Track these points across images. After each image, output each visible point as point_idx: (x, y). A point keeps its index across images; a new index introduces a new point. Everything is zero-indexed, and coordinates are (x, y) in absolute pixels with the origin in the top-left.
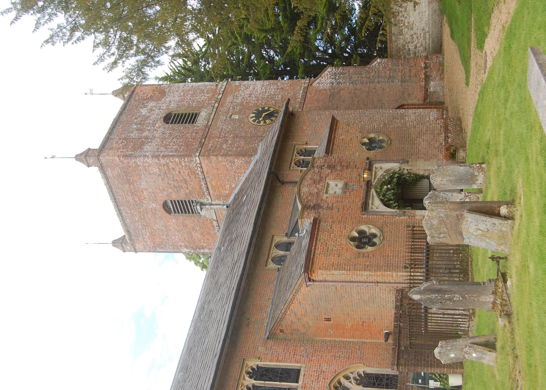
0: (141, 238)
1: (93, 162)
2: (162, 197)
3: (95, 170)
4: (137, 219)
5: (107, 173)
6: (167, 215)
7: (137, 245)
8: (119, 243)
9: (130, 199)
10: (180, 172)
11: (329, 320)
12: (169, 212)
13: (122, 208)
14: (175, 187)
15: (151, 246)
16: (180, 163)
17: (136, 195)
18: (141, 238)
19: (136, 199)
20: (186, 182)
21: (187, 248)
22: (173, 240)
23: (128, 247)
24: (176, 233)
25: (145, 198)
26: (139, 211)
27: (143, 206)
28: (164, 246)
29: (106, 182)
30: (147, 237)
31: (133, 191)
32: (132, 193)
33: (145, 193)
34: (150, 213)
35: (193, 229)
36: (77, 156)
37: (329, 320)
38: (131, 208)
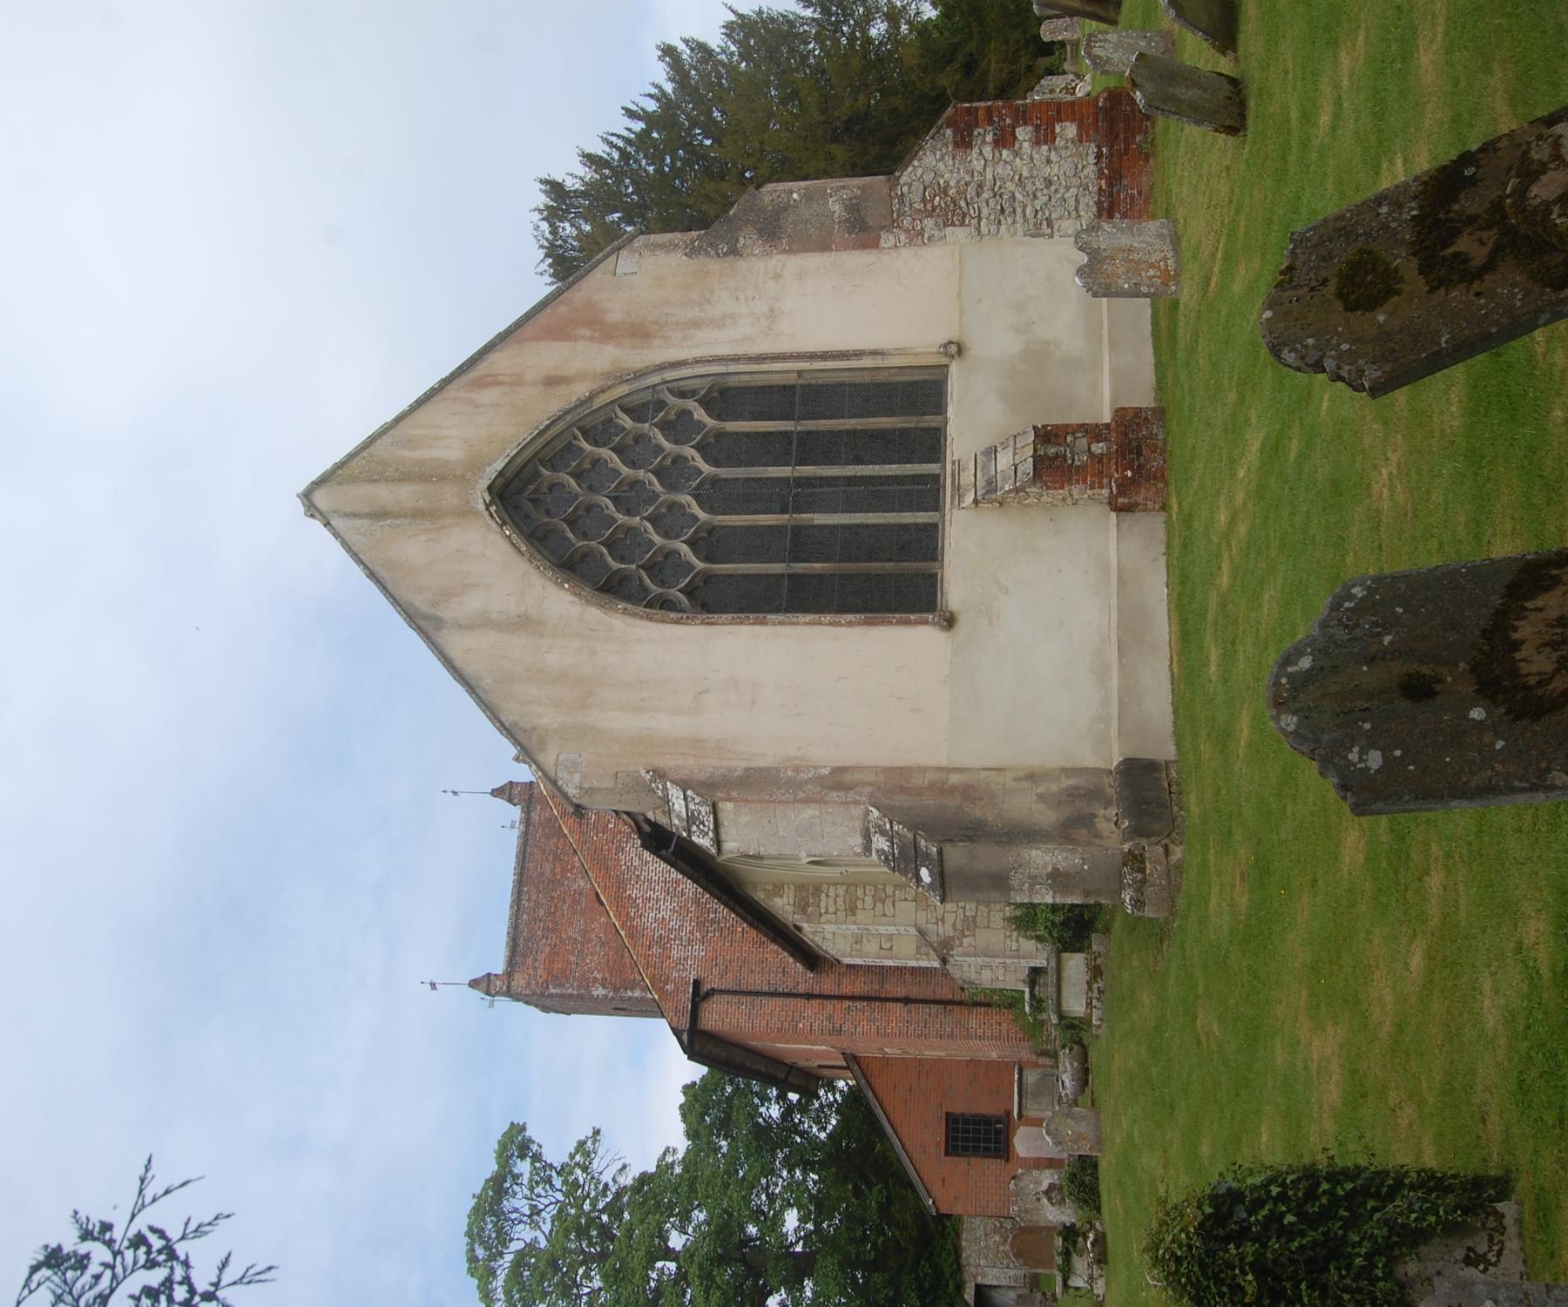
0: (530, 960)
1: (520, 792)
4: (542, 912)
5: (533, 815)
7: (516, 977)
8: (484, 984)
9: (548, 867)
13: (525, 889)
15: (541, 981)
17: (561, 860)
18: (530, 960)
19: (558, 870)
21: (604, 987)
22: (587, 964)
23: (498, 983)
24: (598, 948)
25: (573, 867)
26: (552, 897)
27: (563, 885)
28: (564, 981)
29: (524, 829)
30: (541, 957)
31: (559, 851)
32: (556, 857)
34: (568, 901)
36: (493, 790)
38: (541, 889)
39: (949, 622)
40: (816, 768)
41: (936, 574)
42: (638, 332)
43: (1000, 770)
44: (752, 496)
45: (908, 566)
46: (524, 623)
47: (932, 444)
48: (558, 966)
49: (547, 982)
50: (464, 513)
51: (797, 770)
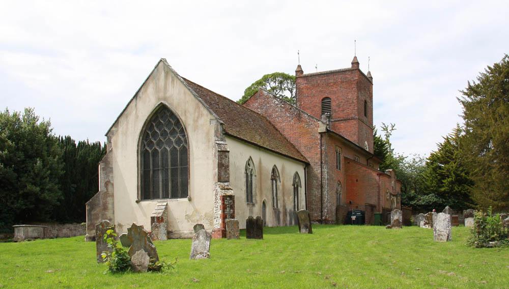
0: (306, 82)
2: (333, 97)
3: (349, 66)
6: (322, 98)
9: (332, 81)
10: (348, 108)
11: (357, 181)
12: (323, 100)
14: (340, 105)
16: (354, 109)
18: (306, 82)
19: (332, 84)
20: (343, 111)
32: (335, 83)
33: (335, 89)
35: (313, 111)
37: (357, 181)
39: (137, 202)
40: (113, 180)
41: (150, 199)
42: (196, 128)
43: (114, 213)
44: (165, 159)
45: (151, 193)
46: (137, 117)
47: (175, 196)
48: (304, 90)
49: (300, 88)
50: (159, 99)
51: (112, 177)
